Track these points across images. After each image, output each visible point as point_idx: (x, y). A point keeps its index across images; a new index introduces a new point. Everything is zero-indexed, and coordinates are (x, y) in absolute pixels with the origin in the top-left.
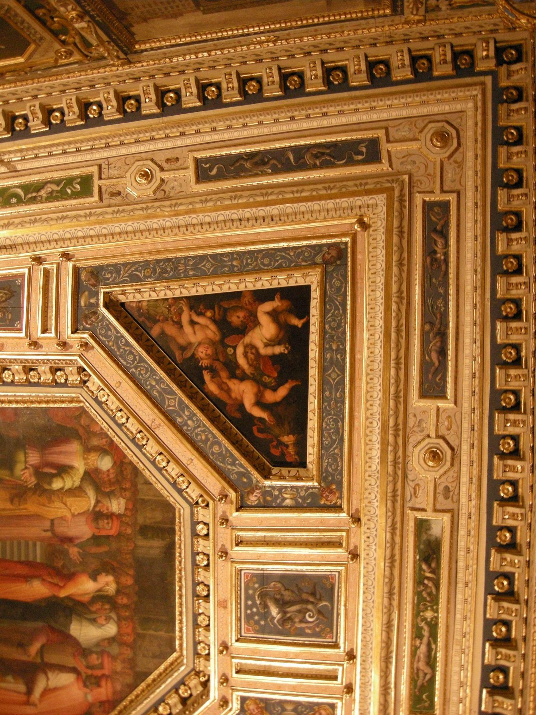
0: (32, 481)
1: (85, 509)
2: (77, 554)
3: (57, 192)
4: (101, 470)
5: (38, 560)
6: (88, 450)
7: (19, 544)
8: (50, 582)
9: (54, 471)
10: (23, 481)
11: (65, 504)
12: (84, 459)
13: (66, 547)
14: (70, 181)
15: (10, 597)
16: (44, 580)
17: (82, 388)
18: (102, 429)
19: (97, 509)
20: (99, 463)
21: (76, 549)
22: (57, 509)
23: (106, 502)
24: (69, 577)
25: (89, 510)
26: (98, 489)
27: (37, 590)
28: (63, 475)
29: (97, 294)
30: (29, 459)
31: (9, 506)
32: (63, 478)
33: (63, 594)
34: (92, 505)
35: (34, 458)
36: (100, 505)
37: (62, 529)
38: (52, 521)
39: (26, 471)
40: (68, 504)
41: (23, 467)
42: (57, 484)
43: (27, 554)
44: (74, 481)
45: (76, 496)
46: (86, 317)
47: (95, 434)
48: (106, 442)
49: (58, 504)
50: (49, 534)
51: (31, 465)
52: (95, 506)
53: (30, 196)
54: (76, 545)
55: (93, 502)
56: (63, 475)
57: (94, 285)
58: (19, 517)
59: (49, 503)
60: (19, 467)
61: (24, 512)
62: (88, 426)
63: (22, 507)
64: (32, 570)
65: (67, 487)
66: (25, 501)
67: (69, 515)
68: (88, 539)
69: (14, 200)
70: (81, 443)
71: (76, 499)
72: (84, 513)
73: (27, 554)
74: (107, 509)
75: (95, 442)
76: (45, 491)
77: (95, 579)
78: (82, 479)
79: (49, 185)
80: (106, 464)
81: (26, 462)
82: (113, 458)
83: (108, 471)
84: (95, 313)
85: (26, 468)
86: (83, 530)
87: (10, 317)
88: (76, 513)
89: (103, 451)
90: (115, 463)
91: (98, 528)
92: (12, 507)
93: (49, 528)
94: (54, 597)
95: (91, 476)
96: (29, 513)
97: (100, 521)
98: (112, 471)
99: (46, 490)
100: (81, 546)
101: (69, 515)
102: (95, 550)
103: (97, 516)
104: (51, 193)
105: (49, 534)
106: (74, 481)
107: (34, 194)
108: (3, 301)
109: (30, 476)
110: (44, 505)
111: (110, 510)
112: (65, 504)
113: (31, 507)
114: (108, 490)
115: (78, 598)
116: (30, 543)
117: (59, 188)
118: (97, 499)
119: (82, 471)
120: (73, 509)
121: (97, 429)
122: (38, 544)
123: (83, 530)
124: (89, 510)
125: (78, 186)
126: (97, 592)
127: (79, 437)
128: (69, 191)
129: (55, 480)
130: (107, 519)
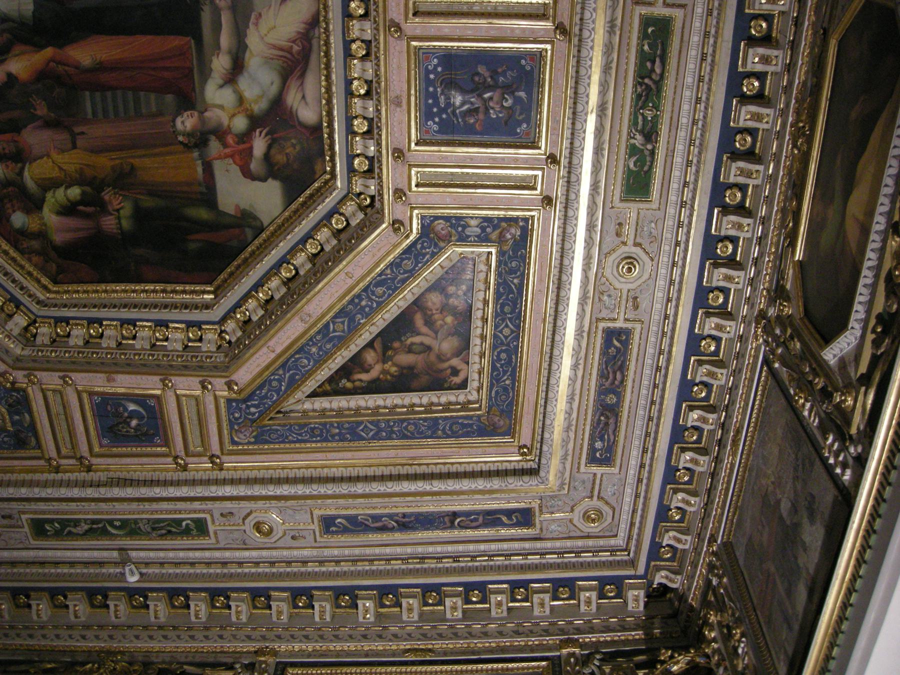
0: (108, 195)
1: (34, 164)
2: (38, 107)
3: (69, 526)
4: (22, 212)
5: (87, 93)
6: (42, 235)
7: (116, 113)
8: (68, 66)
9: (81, 208)
10: (120, 195)
11: (60, 168)
12: (46, 225)
13: (52, 115)
14: (58, 534)
15: (122, 39)
16: (77, 68)
17: (37, 316)
18: (30, 260)
19: (19, 165)
20: (27, 220)
21: (39, 113)
22: (71, 161)
23: (11, 175)
24: (43, 75)
25: (30, 163)
26: (22, 189)
27: (85, 54)
28: (69, 204)
29: (13, 423)
30: (114, 222)
31: (136, 162)
32: (68, 199)
33: (49, 52)
34: (26, 169)
35: (109, 223)
36: (17, 171)
37: (62, 137)
38: (74, 147)
39: (118, 207)
40: (56, 169)
41: (122, 212)
42: (75, 192)
43: (104, 100)
44: (53, 197)
45: (49, 179)
46: (18, 402)
47: (38, 253)
48: (22, 244)
49: (71, 168)
50: (78, 130)
51: (112, 214)
52: (23, 169)
53: (100, 526)
54: (41, 117)
55: (26, 174)
56: (69, 204)
57: (19, 431)
58: (121, 148)
59: (81, 168)
60: (127, 210)
61: (114, 155)
62: (47, 262)
63: (117, 162)
64: (96, 79)
65: (62, 190)
66: (113, 168)
67: (54, 155)
68: (25, 126)
69: (118, 524)
70: (51, 243)
71: (48, 176)
72: (35, 160)
73: (104, 100)
74: (7, 166)
75: (35, 244)
76: (89, 184)
77: (10, 75)
78: (43, 200)
79: (81, 533)
80: (18, 219)
81: (119, 218)
82: (12, 226)
83: (14, 211)
84: (10, 405)
85: (118, 210)
86: (33, 138)
87: (109, 408)
88: (45, 158)
89: (23, 233)
90: (8, 220)
91: (16, 141)
92: (132, 161)
93: (78, 137)
94: (61, 46)
95: (34, 205)
96: (107, 154)
97: (14, 150)
98: (10, 211)
99: (87, 185)
100: (34, 118)
101: (54, 155)
102: (16, 114)
103: (19, 157)
104: (75, 526)
105: (78, 130)
106: (53, 197)
107: (94, 526)
108: (120, 423)
109: (110, 202)
110: (88, 165)
111: (4, 165)
112: (60, 168)
113: (105, 163)
114: (10, 189)
115: (28, 48)
116: (100, 116)
117: (68, 529)
118: (22, 179)
119: (46, 210)
120: (51, 164)
121: (35, 259)
122: (90, 116)
123: (33, 138)
124: (30, 163)
125: (48, 528)
126: (6, 59)
127: (55, 248)
128: (56, 525)
129: (79, 198)
130: (5, 154)
